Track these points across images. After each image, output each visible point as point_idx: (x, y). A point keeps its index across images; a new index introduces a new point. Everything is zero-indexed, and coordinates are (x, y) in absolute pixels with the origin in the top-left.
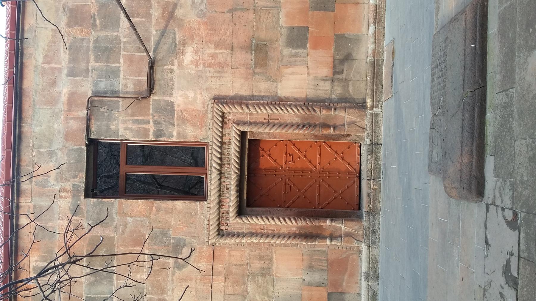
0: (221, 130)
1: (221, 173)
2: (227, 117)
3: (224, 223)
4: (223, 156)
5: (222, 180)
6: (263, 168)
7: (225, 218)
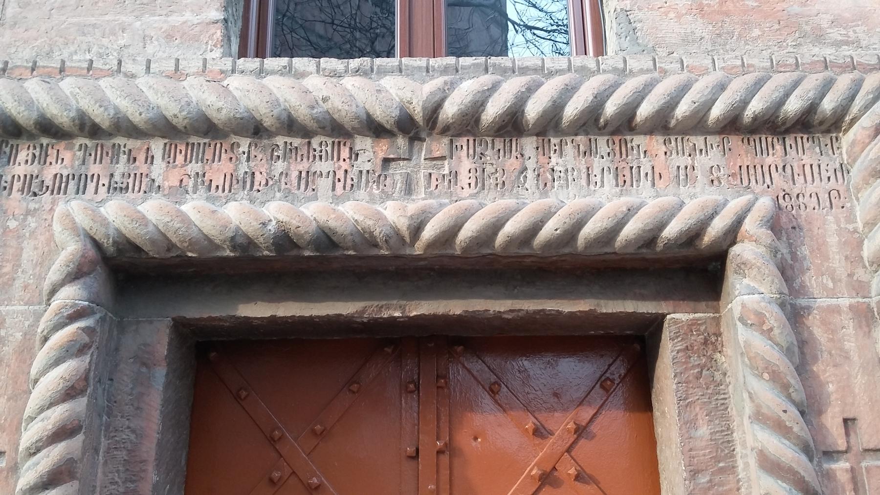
0: (716, 112)
1: (409, 129)
2: (804, 154)
3: (65, 160)
4: (529, 144)
5: (363, 143)
6: (464, 440)
7: (95, 169)
